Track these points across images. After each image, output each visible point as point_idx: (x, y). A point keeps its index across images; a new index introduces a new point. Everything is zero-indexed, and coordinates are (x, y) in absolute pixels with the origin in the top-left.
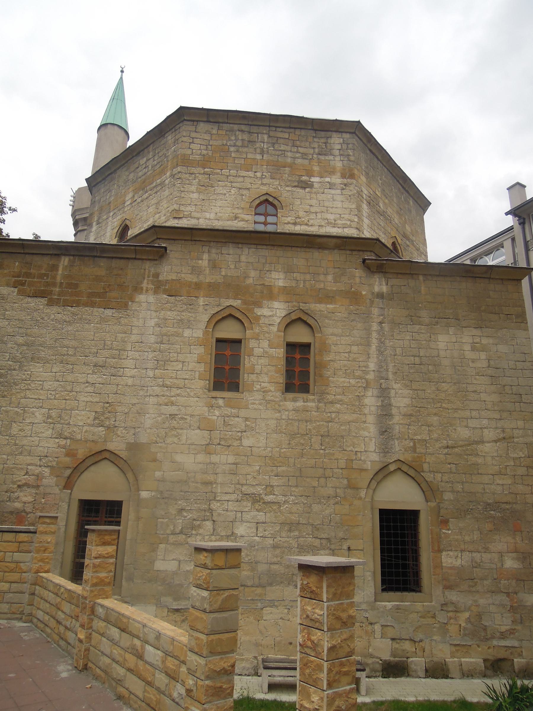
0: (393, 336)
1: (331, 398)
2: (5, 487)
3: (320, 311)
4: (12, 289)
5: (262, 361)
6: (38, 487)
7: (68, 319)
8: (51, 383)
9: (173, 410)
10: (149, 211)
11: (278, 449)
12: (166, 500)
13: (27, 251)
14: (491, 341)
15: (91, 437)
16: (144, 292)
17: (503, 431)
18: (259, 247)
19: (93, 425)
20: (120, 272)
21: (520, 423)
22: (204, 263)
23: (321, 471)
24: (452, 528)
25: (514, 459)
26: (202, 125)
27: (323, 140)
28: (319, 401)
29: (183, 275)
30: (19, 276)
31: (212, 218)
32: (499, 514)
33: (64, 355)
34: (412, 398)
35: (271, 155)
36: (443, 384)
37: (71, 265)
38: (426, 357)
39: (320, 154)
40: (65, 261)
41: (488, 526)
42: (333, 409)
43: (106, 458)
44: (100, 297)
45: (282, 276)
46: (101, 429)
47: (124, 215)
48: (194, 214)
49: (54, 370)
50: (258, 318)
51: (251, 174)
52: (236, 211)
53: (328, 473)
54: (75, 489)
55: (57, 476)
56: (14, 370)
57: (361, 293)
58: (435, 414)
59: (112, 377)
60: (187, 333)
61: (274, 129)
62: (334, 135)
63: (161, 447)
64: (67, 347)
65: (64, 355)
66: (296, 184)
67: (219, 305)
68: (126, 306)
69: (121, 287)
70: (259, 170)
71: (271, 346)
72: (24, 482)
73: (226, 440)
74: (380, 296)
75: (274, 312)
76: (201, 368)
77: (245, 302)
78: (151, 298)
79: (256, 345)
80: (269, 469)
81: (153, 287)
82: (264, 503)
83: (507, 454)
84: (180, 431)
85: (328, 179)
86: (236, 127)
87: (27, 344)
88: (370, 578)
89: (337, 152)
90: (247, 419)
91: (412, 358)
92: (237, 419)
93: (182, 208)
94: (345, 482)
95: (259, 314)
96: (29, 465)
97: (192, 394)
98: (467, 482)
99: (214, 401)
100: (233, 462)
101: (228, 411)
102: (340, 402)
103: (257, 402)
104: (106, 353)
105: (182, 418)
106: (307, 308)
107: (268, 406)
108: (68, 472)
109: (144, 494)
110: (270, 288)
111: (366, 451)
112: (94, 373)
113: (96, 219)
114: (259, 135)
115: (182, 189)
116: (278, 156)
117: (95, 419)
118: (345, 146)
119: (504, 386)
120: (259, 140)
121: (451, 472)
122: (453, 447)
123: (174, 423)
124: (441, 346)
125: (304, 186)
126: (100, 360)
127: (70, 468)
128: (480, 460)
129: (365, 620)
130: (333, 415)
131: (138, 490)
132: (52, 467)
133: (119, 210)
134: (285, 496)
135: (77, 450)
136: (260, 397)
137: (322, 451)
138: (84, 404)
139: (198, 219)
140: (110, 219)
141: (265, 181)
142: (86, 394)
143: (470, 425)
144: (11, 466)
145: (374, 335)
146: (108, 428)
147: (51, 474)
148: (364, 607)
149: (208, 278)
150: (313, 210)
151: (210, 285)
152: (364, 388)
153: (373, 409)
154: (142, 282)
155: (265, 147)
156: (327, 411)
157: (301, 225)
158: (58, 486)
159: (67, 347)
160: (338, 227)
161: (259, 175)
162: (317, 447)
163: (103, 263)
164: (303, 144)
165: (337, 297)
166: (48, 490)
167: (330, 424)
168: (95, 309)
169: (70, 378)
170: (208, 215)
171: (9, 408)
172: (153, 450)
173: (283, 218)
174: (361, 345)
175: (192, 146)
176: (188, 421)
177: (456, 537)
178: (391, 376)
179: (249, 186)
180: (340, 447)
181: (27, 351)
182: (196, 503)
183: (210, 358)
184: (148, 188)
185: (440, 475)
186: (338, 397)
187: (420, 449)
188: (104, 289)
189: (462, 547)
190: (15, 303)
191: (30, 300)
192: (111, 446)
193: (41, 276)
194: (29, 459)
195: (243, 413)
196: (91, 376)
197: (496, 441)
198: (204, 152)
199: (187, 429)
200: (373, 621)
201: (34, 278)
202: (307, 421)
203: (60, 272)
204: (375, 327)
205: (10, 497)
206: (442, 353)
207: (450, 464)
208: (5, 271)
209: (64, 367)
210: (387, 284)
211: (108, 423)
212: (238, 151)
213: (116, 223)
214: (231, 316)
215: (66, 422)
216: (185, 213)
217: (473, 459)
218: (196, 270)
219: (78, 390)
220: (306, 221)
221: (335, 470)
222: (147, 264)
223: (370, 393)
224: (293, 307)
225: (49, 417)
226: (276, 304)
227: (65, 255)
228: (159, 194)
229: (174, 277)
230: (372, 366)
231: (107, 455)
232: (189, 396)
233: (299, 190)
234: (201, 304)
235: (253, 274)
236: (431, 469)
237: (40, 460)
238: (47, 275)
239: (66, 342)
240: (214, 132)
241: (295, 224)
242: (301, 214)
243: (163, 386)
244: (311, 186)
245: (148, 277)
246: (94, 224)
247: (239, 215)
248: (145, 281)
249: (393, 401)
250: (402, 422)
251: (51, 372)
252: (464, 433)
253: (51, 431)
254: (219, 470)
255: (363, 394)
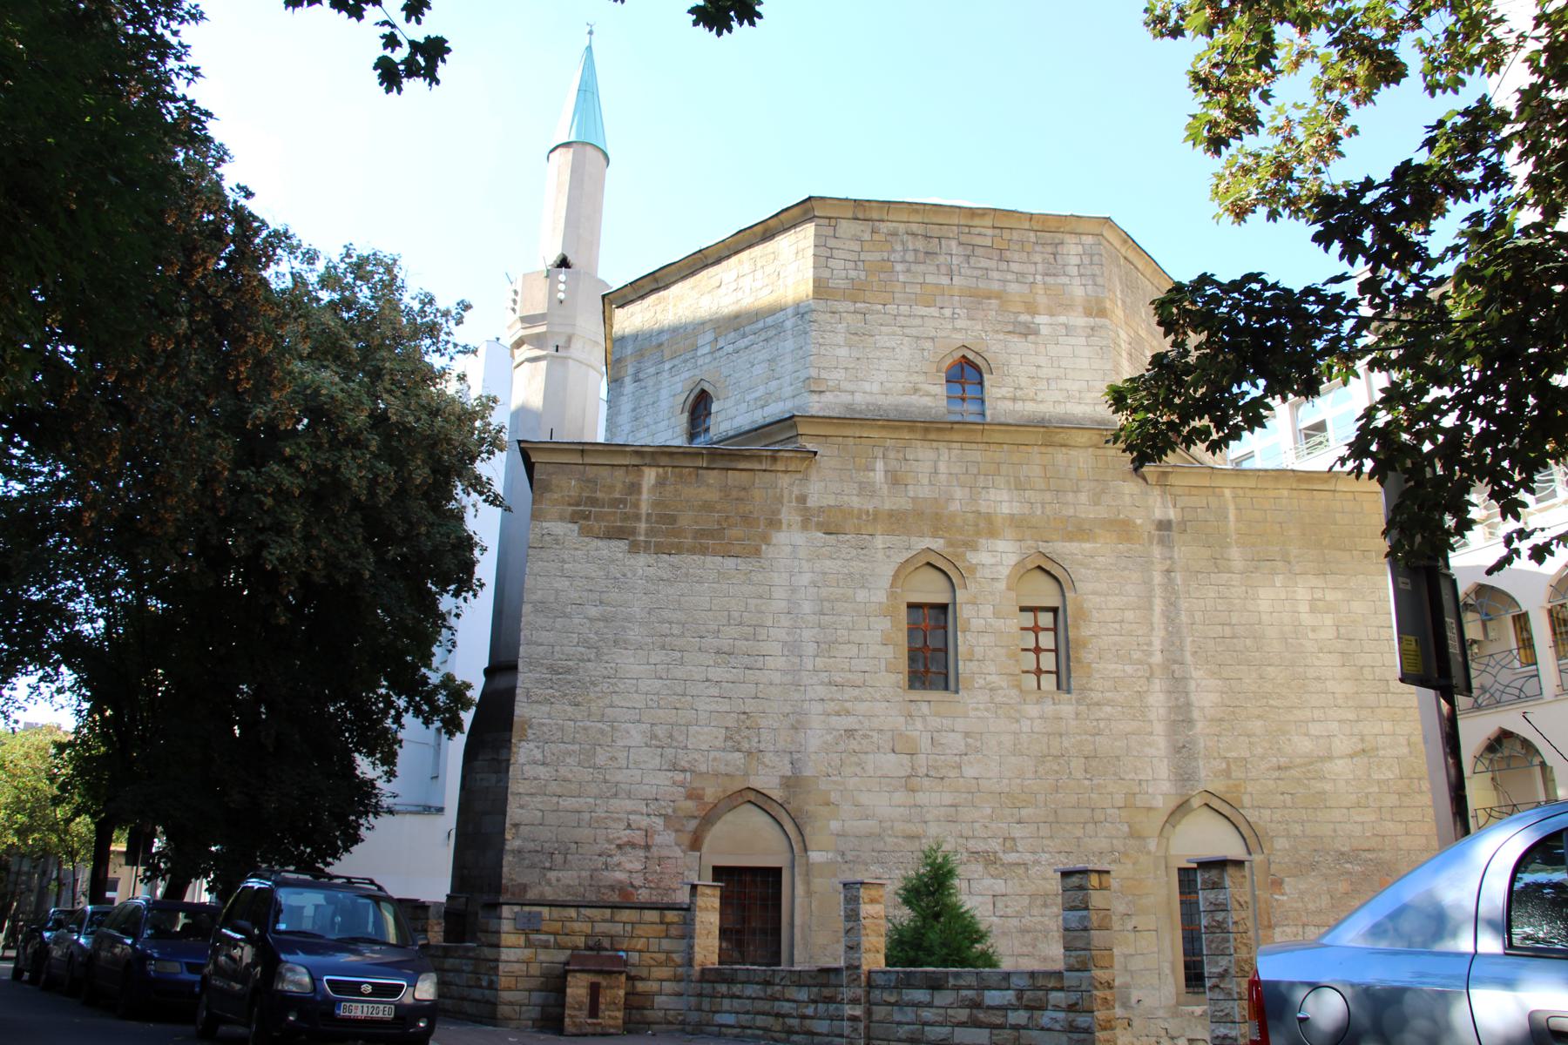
0: (1188, 592)
1: (1096, 696)
2: (597, 848)
3: (1072, 554)
4: (570, 525)
5: (986, 639)
6: (647, 847)
7: (665, 577)
8: (649, 682)
9: (848, 722)
10: (755, 373)
11: (1019, 781)
12: (851, 865)
13: (588, 460)
14: (1339, 595)
15: (722, 769)
16: (784, 527)
17: (1362, 740)
18: (966, 446)
19: (724, 750)
20: (743, 494)
21: (1387, 726)
22: (878, 476)
23: (1087, 813)
24: (1288, 891)
25: (1378, 782)
26: (844, 224)
27: (1049, 249)
28: (1078, 702)
29: (846, 498)
30: (578, 505)
31: (875, 390)
32: (1357, 868)
33: (666, 636)
34: (1222, 692)
35: (966, 276)
36: (1269, 668)
37: (661, 483)
38: (1241, 625)
39: (1047, 275)
40: (650, 476)
41: (1342, 887)
42: (1102, 716)
43: (749, 801)
44: (713, 538)
45: (1004, 495)
46: (737, 755)
47: (697, 372)
48: (844, 385)
49: (652, 661)
50: (973, 569)
51: (933, 311)
52: (915, 378)
53: (1099, 815)
54: (705, 848)
55: (677, 831)
56: (589, 660)
57: (1134, 523)
58: (1259, 717)
59: (747, 671)
60: (861, 595)
61: (967, 230)
62: (1069, 239)
63: (835, 782)
64: (670, 623)
65: (666, 636)
66: (1010, 328)
67: (909, 548)
68: (757, 552)
69: (746, 519)
70: (946, 304)
71: (997, 615)
72: (626, 839)
73: (935, 768)
74: (1164, 525)
75: (998, 559)
76: (888, 653)
77: (950, 544)
78: (799, 538)
79: (974, 614)
80: (1007, 812)
81: (799, 519)
82: (1002, 865)
83: (1369, 776)
84: (863, 756)
85: (1062, 319)
86: (902, 228)
87: (605, 619)
88: (1168, 971)
89: (1074, 271)
90: (967, 735)
91: (1220, 628)
92: (952, 735)
93: (824, 375)
94: (1125, 828)
95: (974, 562)
96: (630, 813)
97: (878, 696)
98: (1309, 821)
99: (913, 706)
100: (950, 802)
101: (935, 722)
102: (1110, 703)
103: (981, 706)
104: (733, 631)
105: (865, 736)
106: (1050, 549)
107: (1000, 712)
108: (693, 824)
109: (815, 856)
110: (989, 518)
111: (1154, 779)
112: (717, 664)
113: (631, 370)
114: (943, 241)
115: (821, 341)
116: (977, 278)
117: (726, 739)
118: (1086, 260)
119: (1362, 667)
120: (944, 251)
121: (1285, 807)
122: (1287, 768)
123: (854, 745)
124: (1264, 606)
125: (1023, 331)
126: (725, 644)
127: (695, 817)
128: (1328, 787)
129: (1163, 1033)
130: (1102, 724)
131: (806, 850)
132: (666, 816)
133: (686, 361)
134: (1033, 853)
135: (703, 789)
136: (987, 698)
137: (1087, 782)
138: (707, 715)
139: (853, 393)
140: (666, 375)
141: (960, 324)
142: (708, 700)
143: (1312, 732)
144: (603, 815)
145: (1158, 591)
146: (749, 753)
147: (666, 827)
148: (1161, 1013)
149: (890, 502)
150: (1043, 373)
151: (891, 514)
152: (1148, 679)
153: (1162, 711)
154: (779, 512)
155: (954, 262)
156: (1092, 717)
157: (1023, 400)
158: (679, 845)
159: (670, 623)
160: (1086, 404)
161: (947, 312)
162: (1079, 774)
163: (712, 477)
164: (1016, 256)
165: (1097, 531)
166: (665, 853)
167: (1097, 738)
168: (709, 559)
169: (679, 672)
170: (867, 386)
171: (588, 724)
172: (823, 787)
173: (994, 390)
174: (1139, 608)
175: (831, 263)
176: (875, 739)
177: (1295, 905)
178: (1189, 658)
179: (933, 334)
180: (1115, 774)
181: (605, 630)
182: (898, 868)
183: (902, 638)
184: (747, 329)
185: (1269, 812)
186: (1108, 695)
187: (1237, 773)
188: (719, 523)
189: (1305, 919)
190: (576, 549)
191: (600, 543)
192: (757, 782)
193: (615, 503)
194: (629, 805)
195: (960, 724)
196: (713, 669)
197: (1351, 757)
198: (853, 274)
199: (874, 753)
200: (1174, 1034)
201: (603, 507)
202: (1061, 735)
203: (645, 495)
204: (1158, 578)
205: (606, 864)
206: (1265, 617)
207: (1283, 794)
208: (556, 496)
209: (667, 655)
210: (1175, 506)
211: (747, 746)
212: (908, 271)
213: (680, 385)
214: (929, 564)
215: (682, 745)
216: (830, 383)
217: (1318, 785)
218: (865, 489)
219: (695, 693)
220: (1032, 394)
221: (1109, 811)
222: (784, 481)
223: (1157, 685)
224: (1027, 548)
225: (654, 736)
226: (1001, 545)
227: (650, 466)
228: (772, 343)
229: (830, 500)
230: (1157, 644)
231: (752, 796)
232: (874, 700)
233: (1015, 339)
234: (881, 546)
235: (959, 493)
236: (1255, 804)
237: (647, 805)
238: (623, 501)
239: (666, 614)
240: (867, 236)
241: (1014, 399)
242: (1024, 381)
243: (830, 683)
244: (1036, 333)
245: (790, 502)
246: (628, 380)
247: (920, 386)
248: (784, 510)
249: (1193, 697)
250: (1208, 731)
251: (648, 664)
252: (1304, 745)
253: (658, 759)
254: (929, 817)
255: (1145, 688)
